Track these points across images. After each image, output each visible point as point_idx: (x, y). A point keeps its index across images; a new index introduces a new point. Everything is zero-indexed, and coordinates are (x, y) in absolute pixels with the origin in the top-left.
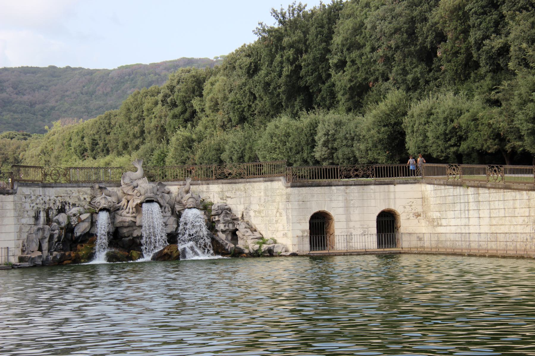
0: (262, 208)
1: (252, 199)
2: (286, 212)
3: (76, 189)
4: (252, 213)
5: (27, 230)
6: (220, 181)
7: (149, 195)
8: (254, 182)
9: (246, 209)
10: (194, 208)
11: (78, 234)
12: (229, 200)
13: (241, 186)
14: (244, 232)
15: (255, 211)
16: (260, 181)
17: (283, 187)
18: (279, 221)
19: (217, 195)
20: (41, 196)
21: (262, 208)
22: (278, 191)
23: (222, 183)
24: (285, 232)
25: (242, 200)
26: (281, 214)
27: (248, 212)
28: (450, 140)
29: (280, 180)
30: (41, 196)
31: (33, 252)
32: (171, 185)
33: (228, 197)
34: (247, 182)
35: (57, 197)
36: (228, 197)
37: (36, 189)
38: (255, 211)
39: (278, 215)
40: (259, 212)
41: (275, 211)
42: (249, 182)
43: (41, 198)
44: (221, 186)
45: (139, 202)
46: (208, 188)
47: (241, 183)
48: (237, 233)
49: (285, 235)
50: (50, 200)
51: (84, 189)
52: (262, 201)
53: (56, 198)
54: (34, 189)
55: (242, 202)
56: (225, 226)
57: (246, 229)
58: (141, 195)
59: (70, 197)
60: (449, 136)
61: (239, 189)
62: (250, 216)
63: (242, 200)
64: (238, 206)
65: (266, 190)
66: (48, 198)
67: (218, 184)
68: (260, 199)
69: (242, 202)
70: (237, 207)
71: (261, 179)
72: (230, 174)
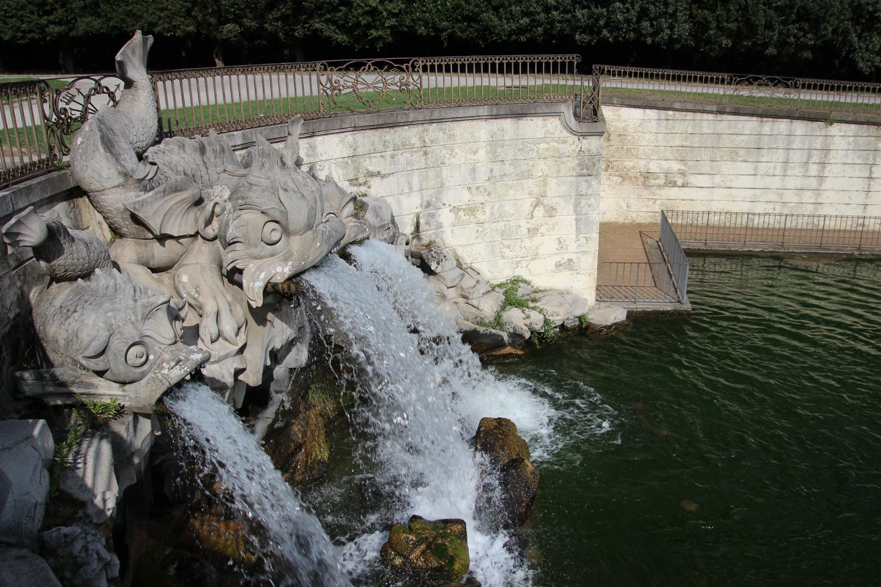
0: (481, 198)
1: (445, 172)
2: (577, 205)
4: (445, 217)
8: (455, 119)
9: (428, 205)
12: (375, 182)
13: (411, 134)
14: (454, 280)
15: (455, 210)
16: (477, 118)
17: (565, 133)
18: (543, 230)
19: (340, 172)
21: (481, 198)
22: (541, 146)
23: (356, 129)
24: (566, 257)
25: (416, 179)
26: (551, 211)
27: (432, 216)
28: (49, 13)
29: (558, 114)
33: (372, 175)
34: (431, 121)
36: (372, 175)
38: (455, 210)
39: (539, 212)
40: (471, 210)
41: (527, 204)
42: (440, 121)
44: (349, 137)
45: (281, 272)
46: (312, 148)
49: (569, 265)
52: (482, 177)
55: (416, 186)
58: (286, 231)
60: (48, 8)
61: (405, 146)
62: (440, 226)
63: (416, 179)
64: (403, 198)
65: (494, 143)
67: (342, 130)
68: (474, 170)
69: (416, 186)
70: (399, 203)
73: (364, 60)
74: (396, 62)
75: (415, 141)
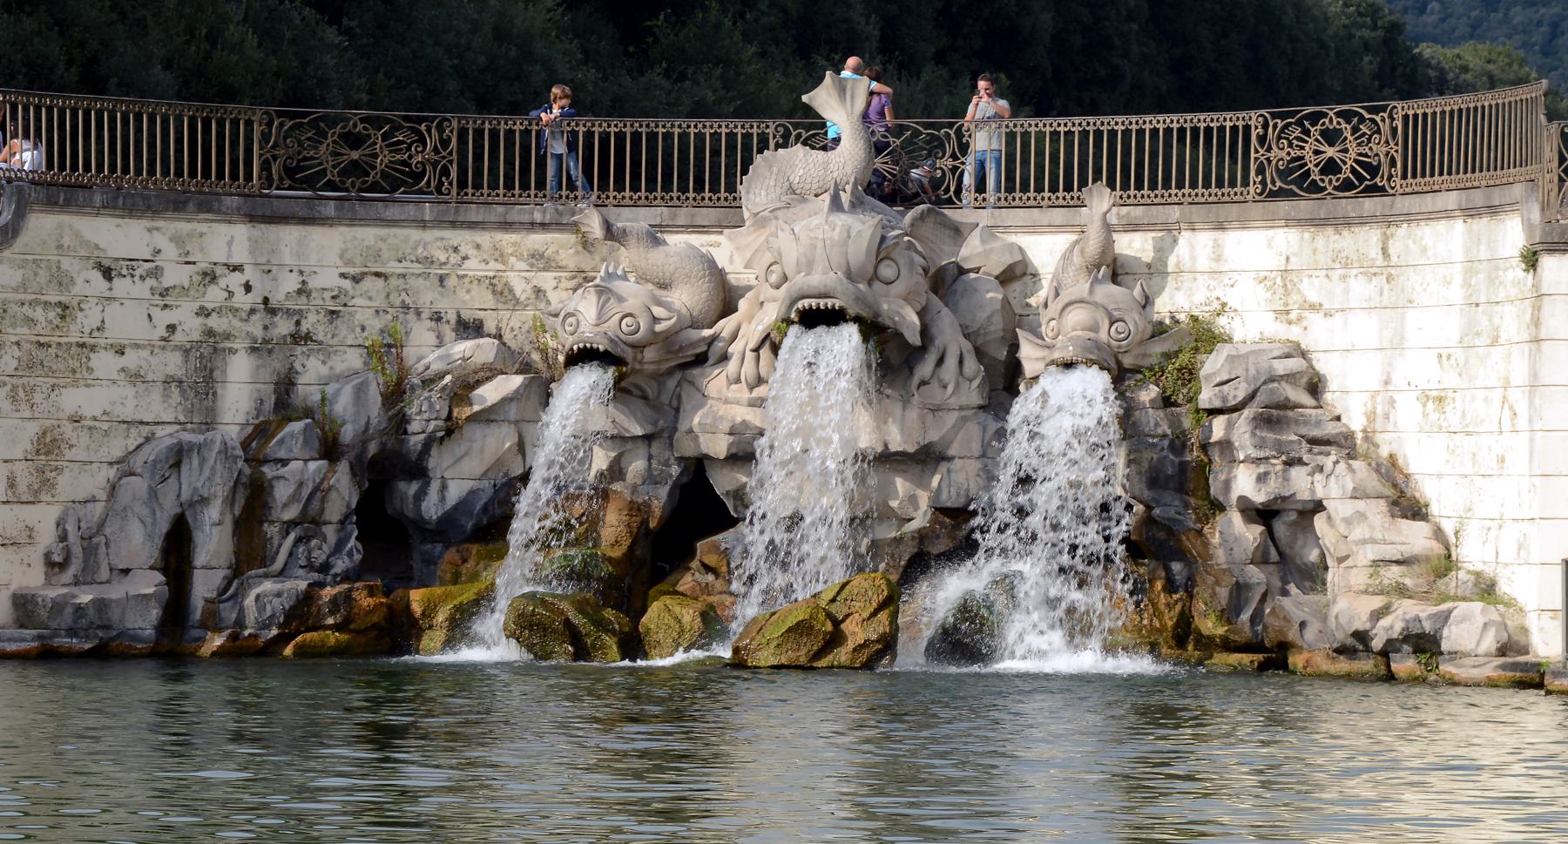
3: (484, 238)
5: (117, 453)
6: (1284, 206)
7: (819, 278)
10: (1089, 363)
11: (456, 492)
12: (1314, 318)
20: (237, 268)
23: (1291, 222)
30: (237, 268)
31: (126, 571)
32: (1033, 229)
33: (1313, 307)
35: (356, 279)
36: (1313, 307)
37: (203, 227)
43: (235, 281)
47: (1363, 221)
48: (1319, 521)
50: (303, 291)
51: (537, 240)
53: (347, 284)
54: (183, 227)
56: (1262, 478)
57: (1361, 505)
59: (442, 279)
66: (291, 283)
67: (1270, 221)
71: (1451, 200)
72: (1331, 167)
73: (1323, 109)
74: (1371, 110)
75: (1375, 252)
